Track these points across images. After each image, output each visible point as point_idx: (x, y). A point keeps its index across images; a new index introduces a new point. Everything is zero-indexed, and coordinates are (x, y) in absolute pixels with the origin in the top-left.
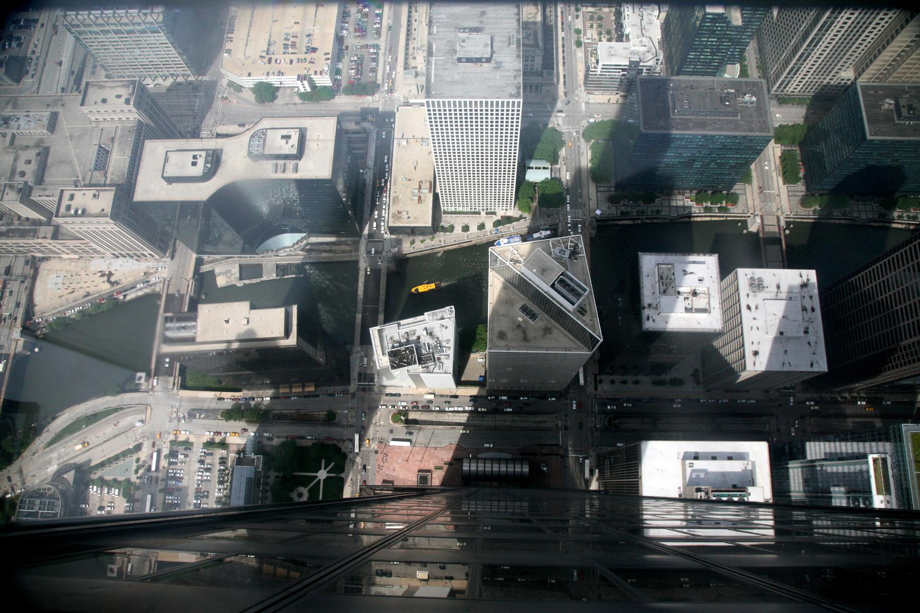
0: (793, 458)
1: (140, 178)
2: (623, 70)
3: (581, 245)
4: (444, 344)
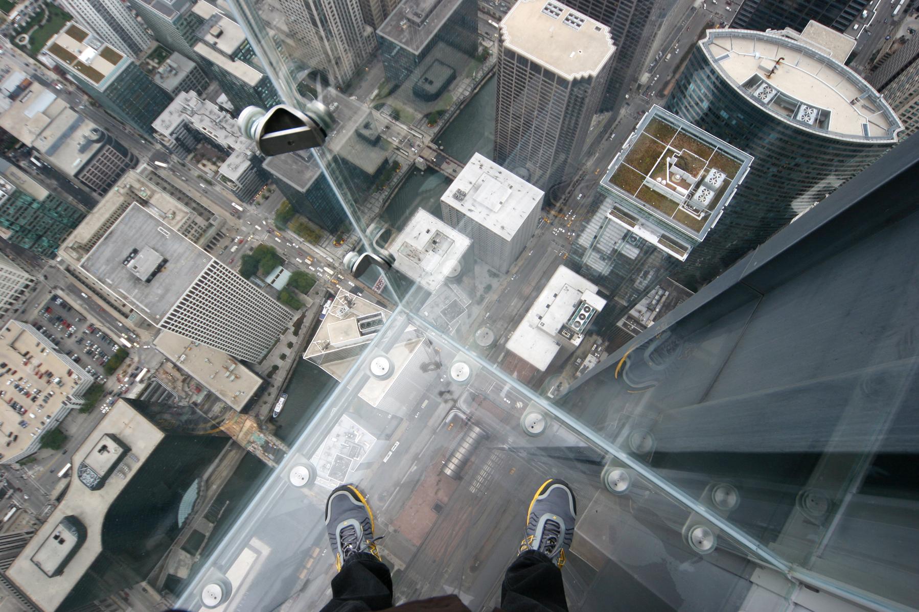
0: (581, 255)
1: (34, 598)
2: (252, 169)
3: (348, 294)
4: (351, 431)
